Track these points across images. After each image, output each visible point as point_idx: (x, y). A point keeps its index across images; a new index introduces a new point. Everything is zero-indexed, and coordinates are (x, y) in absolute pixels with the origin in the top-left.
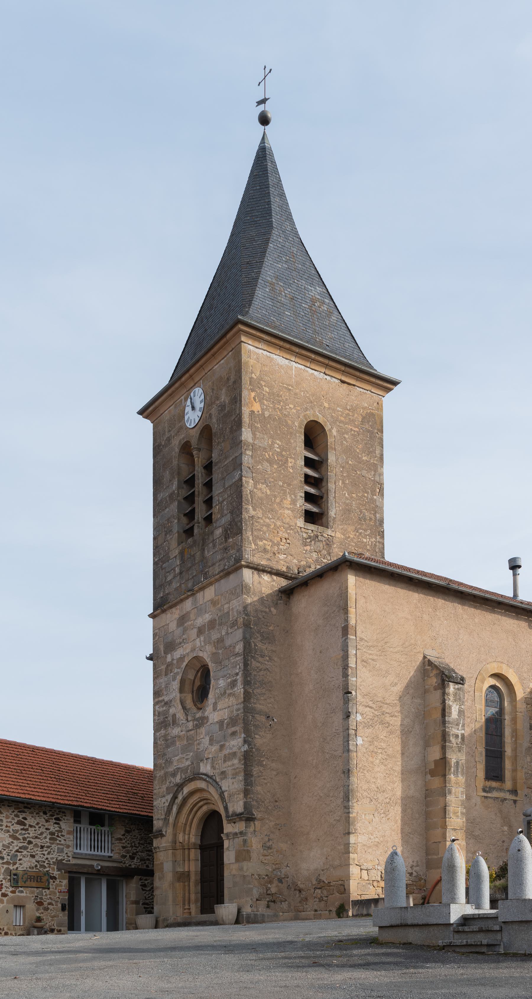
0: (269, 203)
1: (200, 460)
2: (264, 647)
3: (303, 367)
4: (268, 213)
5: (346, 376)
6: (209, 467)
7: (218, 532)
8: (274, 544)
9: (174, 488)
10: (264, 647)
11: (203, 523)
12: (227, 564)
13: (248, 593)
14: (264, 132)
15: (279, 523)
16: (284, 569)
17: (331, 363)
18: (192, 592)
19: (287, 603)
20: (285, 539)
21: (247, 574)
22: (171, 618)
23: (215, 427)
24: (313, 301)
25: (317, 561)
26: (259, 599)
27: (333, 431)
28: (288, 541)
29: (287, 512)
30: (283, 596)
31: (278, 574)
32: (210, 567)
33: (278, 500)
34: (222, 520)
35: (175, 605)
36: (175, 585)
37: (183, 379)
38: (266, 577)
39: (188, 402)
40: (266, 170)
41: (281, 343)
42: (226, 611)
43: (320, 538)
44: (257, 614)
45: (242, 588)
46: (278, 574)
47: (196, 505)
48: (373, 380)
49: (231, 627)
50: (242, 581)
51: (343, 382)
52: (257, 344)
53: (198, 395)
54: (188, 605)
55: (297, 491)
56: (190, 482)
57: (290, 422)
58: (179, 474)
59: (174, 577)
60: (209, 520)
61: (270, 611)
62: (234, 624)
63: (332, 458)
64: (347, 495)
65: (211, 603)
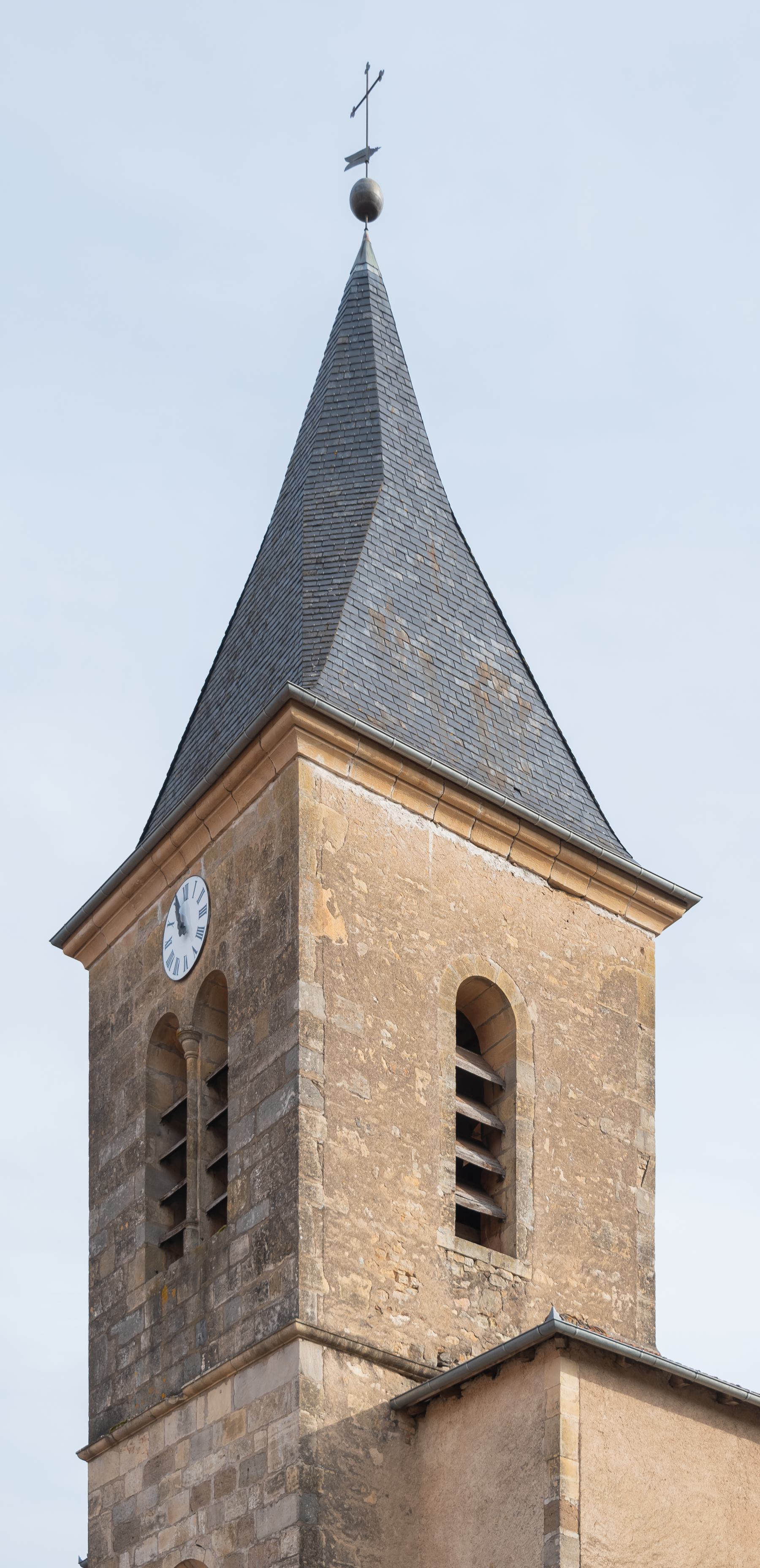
0: (374, 415)
1: (198, 1064)
2: (352, 1547)
4: (371, 439)
5: (564, 872)
6: (219, 1082)
7: (241, 1246)
8: (377, 1287)
9: (137, 1132)
10: (352, 1547)
11: (206, 1223)
12: (261, 1327)
13: (312, 1405)
14: (365, 236)
15: (390, 1233)
16: (404, 1352)
18: (179, 1399)
19: (410, 1439)
20: (408, 1275)
21: (310, 1357)
22: (130, 1460)
23: (234, 980)
24: (483, 674)
25: (486, 1337)
26: (339, 1424)
27: (529, 1009)
28: (414, 1281)
29: (411, 1205)
30: (400, 1419)
31: (390, 1362)
32: (220, 1335)
33: (389, 1173)
34: (250, 1216)
35: (138, 1430)
36: (139, 1379)
37: (159, 854)
38: (358, 1369)
39: (172, 917)
40: (367, 332)
42: (258, 1448)
44: (335, 1462)
45: (297, 1392)
46: (390, 1362)
47: (189, 1180)
49: (271, 1491)
50: (298, 1373)
51: (555, 886)
53: (194, 897)
54: (169, 1429)
55: (437, 1155)
56: (176, 1119)
58: (149, 1098)
59: (138, 1359)
60: (218, 1214)
61: (368, 1455)
62: (278, 1482)
63: (525, 1079)
65: (224, 1427)
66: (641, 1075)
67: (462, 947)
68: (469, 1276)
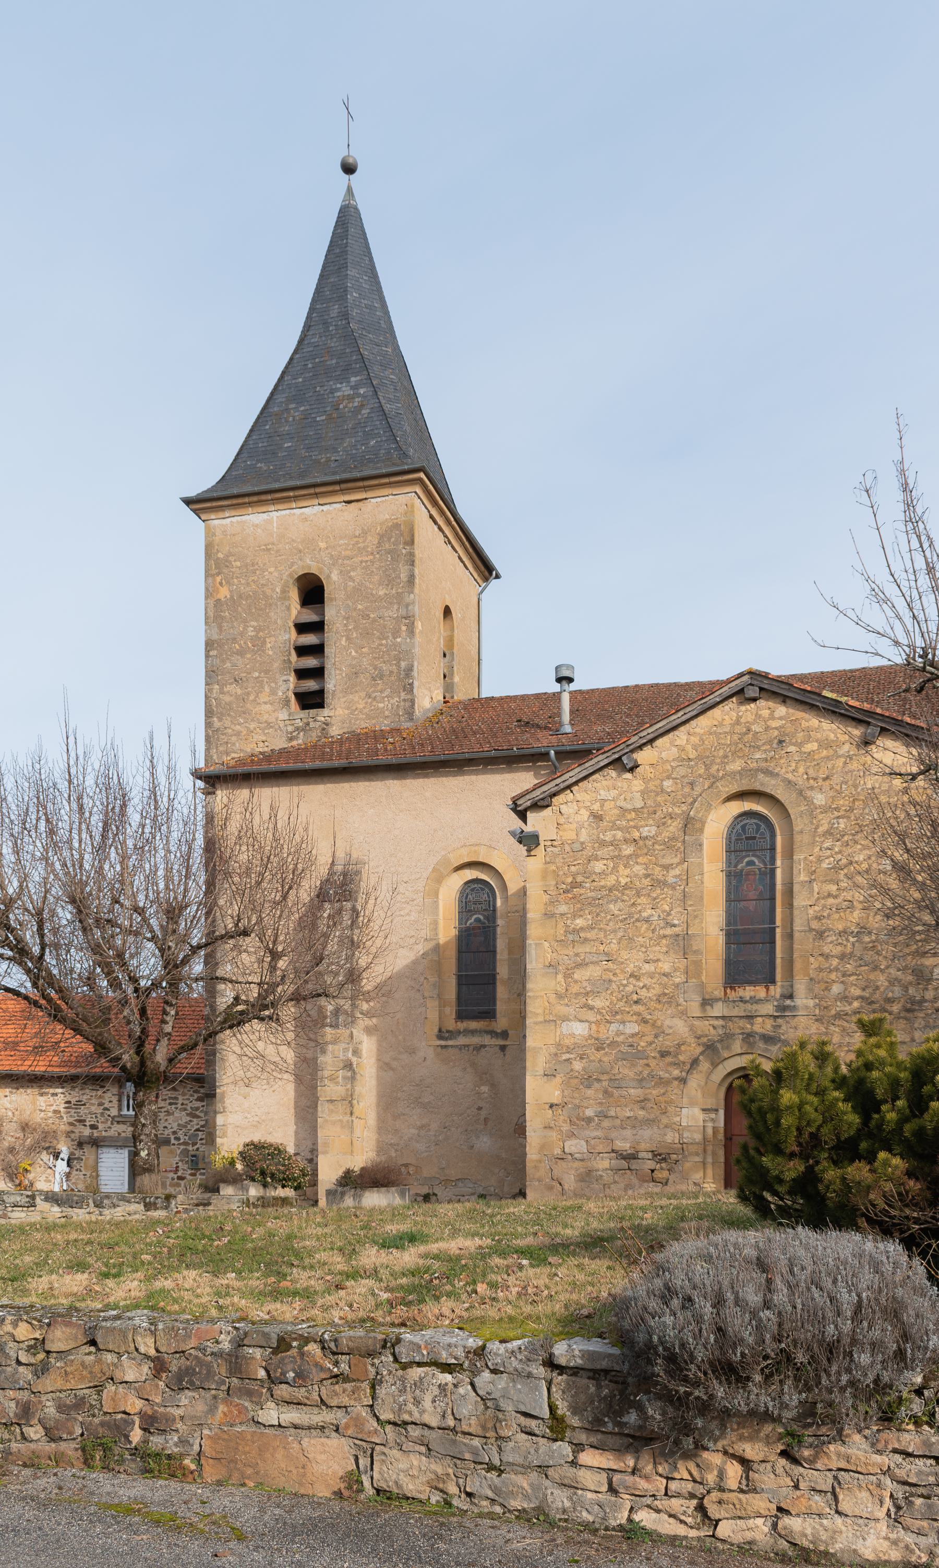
3: (288, 512)
15: (252, 726)
17: (318, 490)
41: (246, 500)
43: (312, 725)
48: (386, 480)
52: (221, 515)
55: (278, 676)
57: (269, 592)
64: (354, 653)
66: (404, 576)
67: (293, 564)
68: (297, 729)
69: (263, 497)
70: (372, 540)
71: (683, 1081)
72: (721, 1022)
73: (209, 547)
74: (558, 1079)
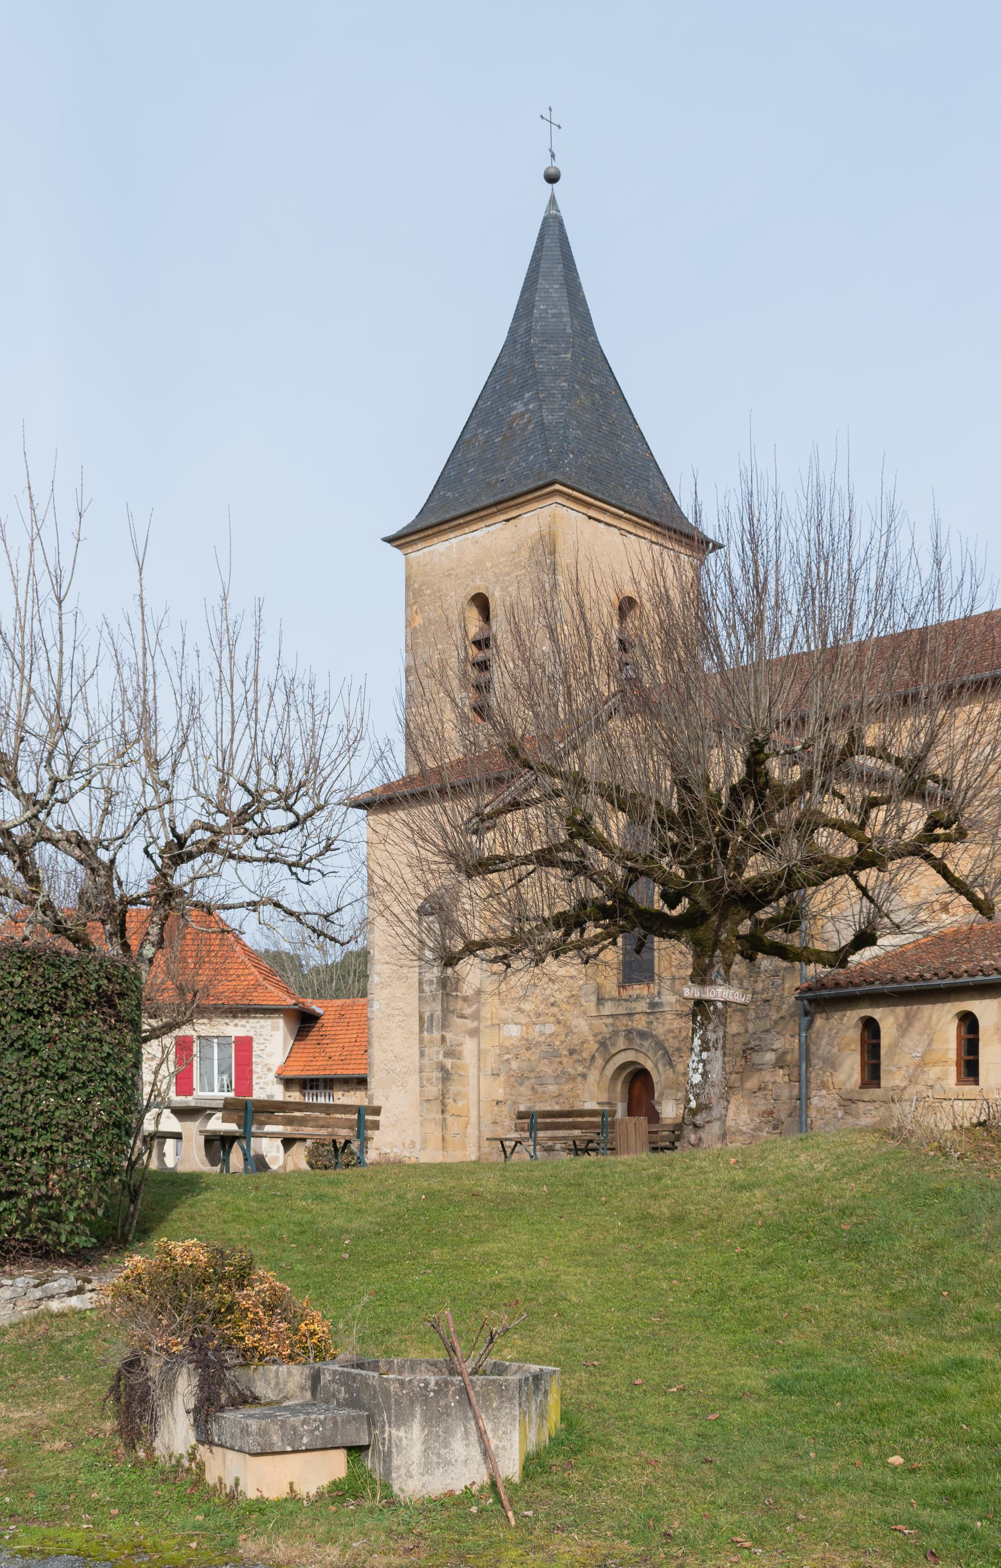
17: (482, 514)
41: (430, 532)
52: (415, 548)
69: (442, 527)
70: (525, 553)
71: (584, 1076)
72: (610, 1020)
73: (408, 579)
74: (502, 1078)
